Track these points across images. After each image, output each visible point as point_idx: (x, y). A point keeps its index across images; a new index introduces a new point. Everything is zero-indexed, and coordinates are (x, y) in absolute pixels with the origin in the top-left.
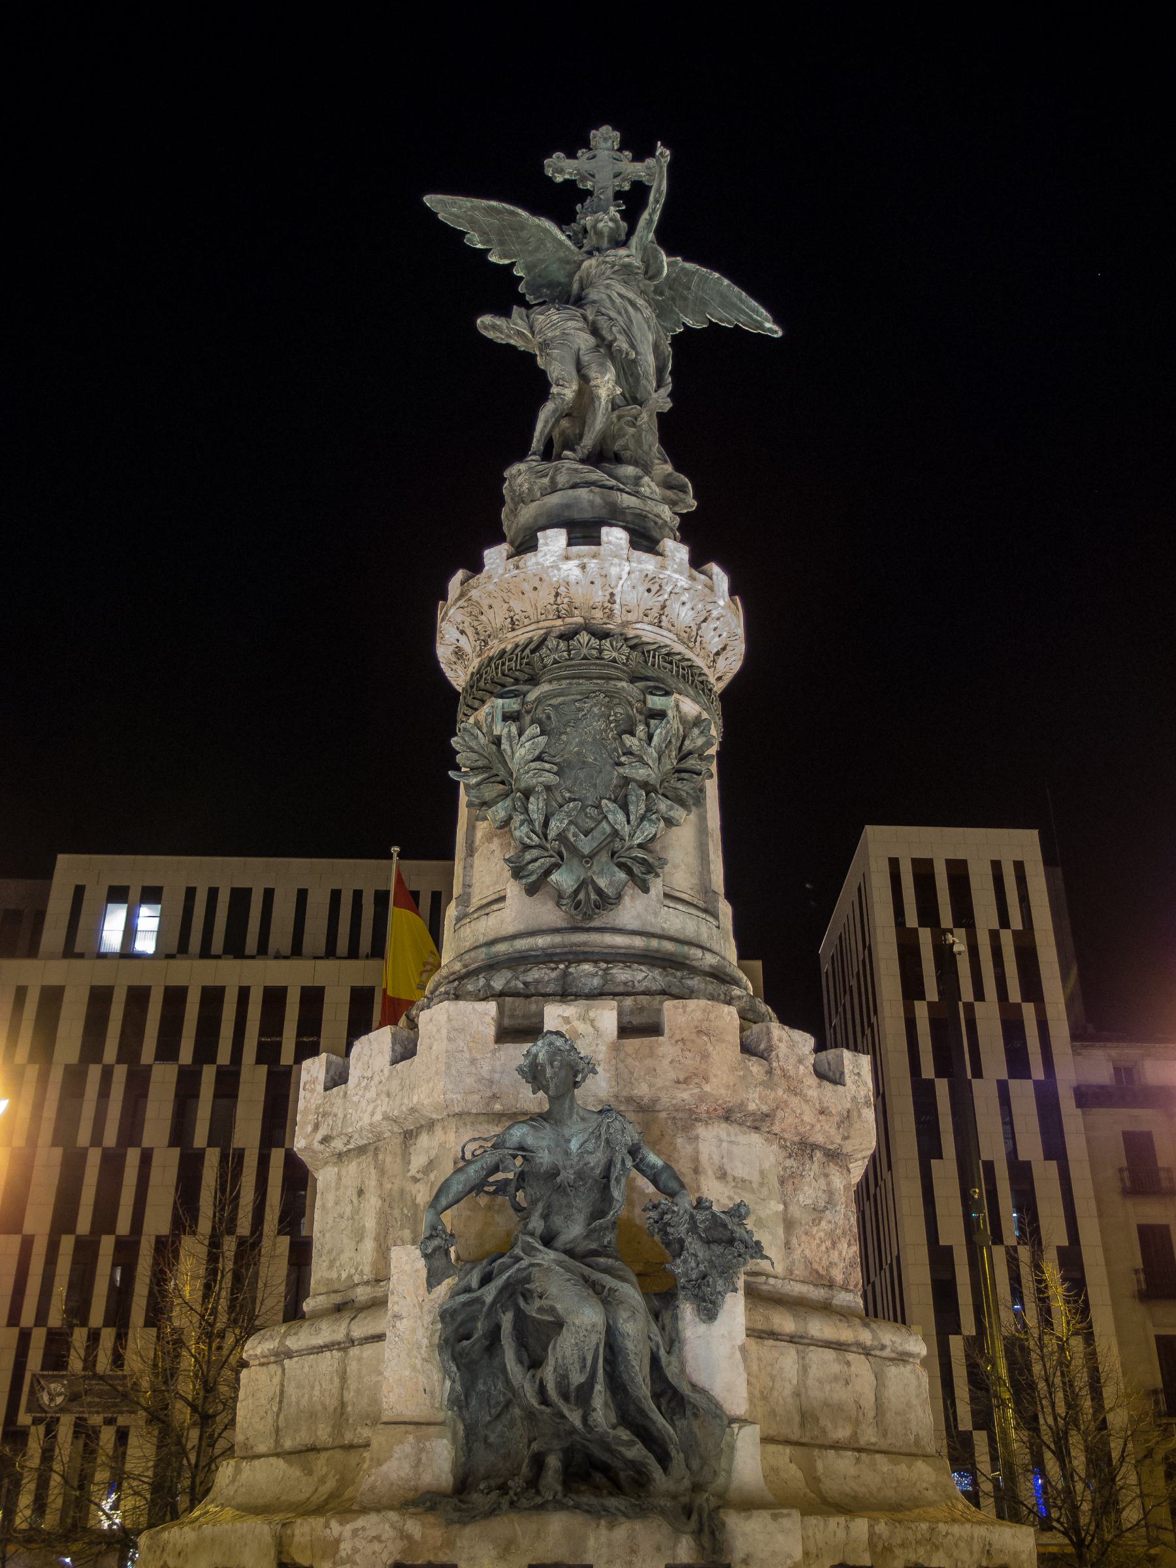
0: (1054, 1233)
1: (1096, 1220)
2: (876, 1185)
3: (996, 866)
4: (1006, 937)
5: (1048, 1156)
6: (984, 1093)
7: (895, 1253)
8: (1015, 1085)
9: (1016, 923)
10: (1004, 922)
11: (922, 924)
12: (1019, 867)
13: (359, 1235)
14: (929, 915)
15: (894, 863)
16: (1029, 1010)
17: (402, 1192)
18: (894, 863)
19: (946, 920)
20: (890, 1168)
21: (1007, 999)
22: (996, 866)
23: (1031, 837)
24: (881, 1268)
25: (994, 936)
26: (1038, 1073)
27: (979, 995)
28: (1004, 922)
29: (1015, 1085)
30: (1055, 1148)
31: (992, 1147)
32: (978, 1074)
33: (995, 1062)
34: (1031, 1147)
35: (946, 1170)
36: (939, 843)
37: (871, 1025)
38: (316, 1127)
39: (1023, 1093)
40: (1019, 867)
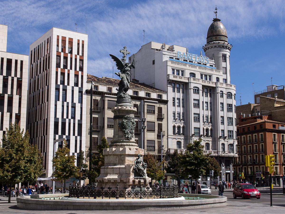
0: (78, 117)
1: (86, 115)
2: (42, 103)
3: (79, 41)
4: (78, 57)
5: (79, 103)
6: (69, 89)
7: (46, 118)
8: (75, 87)
9: (81, 54)
10: (78, 54)
11: (62, 51)
12: (83, 41)
13: (116, 161)
14: (63, 50)
15: (58, 36)
16: (80, 73)
17: (121, 159)
18: (58, 36)
19: (67, 51)
20: (48, 101)
21: (76, 70)
22: (79, 41)
23: (86, 36)
24: (41, 119)
25: (76, 56)
26: (80, 86)
27: (71, 68)
28: (78, 54)
29: (75, 87)
30: (81, 101)
31: (69, 99)
32: (68, 84)
33: (72, 83)
34: (76, 100)
35: (59, 103)
36: (68, 34)
37: (46, 69)
38: (112, 153)
39: (76, 89)
40: (83, 41)
